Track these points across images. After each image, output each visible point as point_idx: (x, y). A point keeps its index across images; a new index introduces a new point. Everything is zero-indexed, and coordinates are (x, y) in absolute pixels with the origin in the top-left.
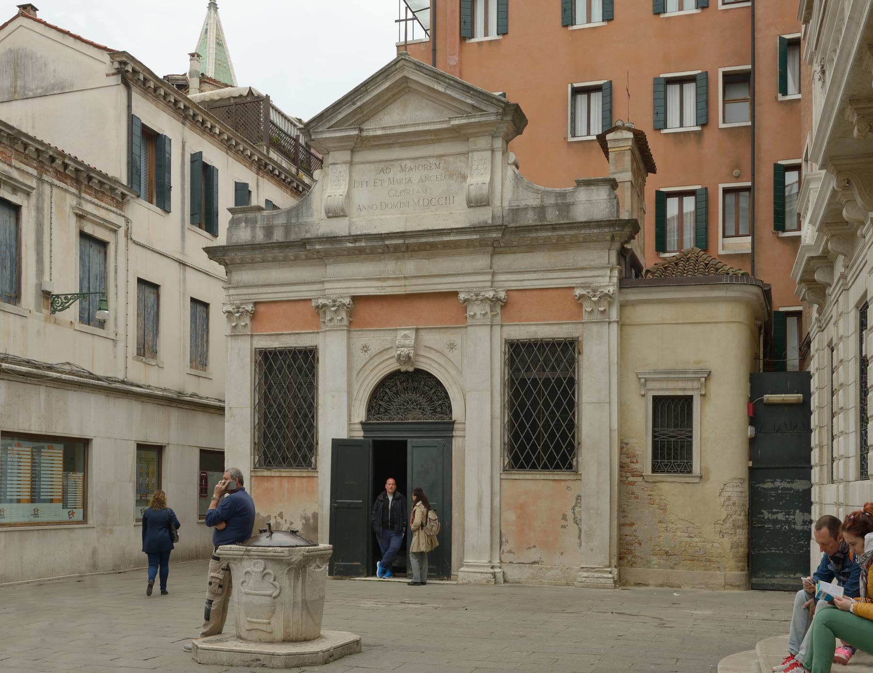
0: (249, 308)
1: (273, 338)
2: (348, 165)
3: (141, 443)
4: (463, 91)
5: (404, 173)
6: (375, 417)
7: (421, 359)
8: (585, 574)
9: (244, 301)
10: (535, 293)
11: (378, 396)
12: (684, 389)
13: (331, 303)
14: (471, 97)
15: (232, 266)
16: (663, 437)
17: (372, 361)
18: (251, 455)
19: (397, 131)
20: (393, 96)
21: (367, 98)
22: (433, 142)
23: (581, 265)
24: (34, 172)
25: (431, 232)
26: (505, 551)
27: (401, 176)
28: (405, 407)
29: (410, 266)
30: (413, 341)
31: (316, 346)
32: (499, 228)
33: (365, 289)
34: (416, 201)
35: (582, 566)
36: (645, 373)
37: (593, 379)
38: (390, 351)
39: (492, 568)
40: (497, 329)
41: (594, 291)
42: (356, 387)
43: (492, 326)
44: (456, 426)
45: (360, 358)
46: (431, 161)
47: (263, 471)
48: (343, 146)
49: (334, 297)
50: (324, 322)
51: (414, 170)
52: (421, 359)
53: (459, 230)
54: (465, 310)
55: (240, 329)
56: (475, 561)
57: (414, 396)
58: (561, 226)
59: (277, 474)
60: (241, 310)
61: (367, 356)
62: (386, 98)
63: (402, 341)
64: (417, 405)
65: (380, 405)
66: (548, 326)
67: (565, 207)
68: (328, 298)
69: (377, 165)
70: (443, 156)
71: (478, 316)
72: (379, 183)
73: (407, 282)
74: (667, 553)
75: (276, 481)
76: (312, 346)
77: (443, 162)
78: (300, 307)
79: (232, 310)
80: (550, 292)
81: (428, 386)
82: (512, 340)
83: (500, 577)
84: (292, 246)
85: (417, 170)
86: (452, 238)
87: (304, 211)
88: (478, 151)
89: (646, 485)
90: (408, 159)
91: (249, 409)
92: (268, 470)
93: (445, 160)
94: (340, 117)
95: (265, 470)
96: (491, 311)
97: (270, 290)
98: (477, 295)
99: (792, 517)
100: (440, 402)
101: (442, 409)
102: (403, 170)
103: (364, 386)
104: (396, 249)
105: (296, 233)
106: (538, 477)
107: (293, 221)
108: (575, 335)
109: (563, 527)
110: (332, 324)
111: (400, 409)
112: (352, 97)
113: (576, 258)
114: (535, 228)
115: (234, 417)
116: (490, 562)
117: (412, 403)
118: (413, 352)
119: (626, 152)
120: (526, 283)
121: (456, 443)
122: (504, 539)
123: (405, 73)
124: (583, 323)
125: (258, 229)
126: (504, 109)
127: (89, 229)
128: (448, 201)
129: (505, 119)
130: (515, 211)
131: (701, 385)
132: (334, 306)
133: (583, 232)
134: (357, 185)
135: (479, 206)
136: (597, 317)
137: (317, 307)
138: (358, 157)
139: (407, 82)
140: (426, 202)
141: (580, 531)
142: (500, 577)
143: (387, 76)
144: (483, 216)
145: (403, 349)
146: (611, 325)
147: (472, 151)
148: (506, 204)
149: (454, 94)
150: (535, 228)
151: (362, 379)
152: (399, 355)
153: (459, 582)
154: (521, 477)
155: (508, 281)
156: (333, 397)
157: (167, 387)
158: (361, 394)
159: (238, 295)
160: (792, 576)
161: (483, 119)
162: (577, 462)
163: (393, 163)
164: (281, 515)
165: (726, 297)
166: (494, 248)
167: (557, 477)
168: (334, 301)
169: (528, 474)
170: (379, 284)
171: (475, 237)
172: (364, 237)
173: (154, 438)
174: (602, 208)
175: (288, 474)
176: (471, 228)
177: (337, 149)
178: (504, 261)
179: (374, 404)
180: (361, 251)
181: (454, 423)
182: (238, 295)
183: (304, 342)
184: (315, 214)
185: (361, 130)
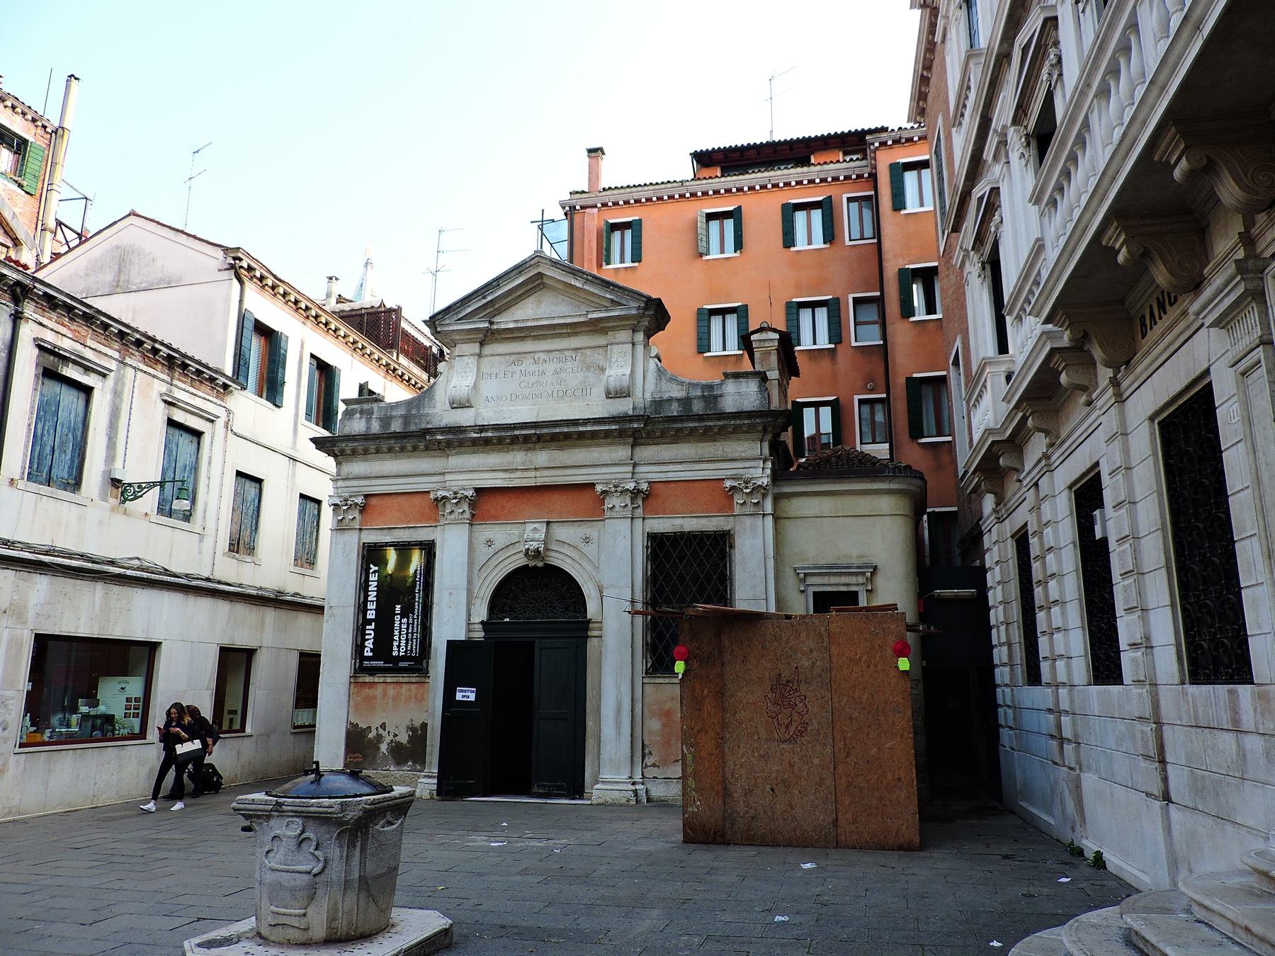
0: (360, 500)
1: (385, 532)
2: (476, 357)
7: (552, 554)
9: (353, 494)
12: (848, 585)
18: (352, 659)
19: (529, 324)
20: (527, 291)
21: (500, 292)
22: (569, 335)
23: (731, 456)
24: (116, 355)
27: (533, 368)
34: (550, 393)
38: (517, 544)
39: (633, 784)
40: (638, 522)
41: (746, 483)
42: (477, 583)
43: (632, 518)
44: (591, 625)
45: (483, 553)
46: (567, 353)
48: (472, 339)
49: (455, 489)
50: (443, 515)
52: (552, 554)
60: (349, 502)
61: (491, 551)
68: (448, 490)
69: (507, 357)
70: (580, 349)
71: (617, 508)
72: (510, 375)
73: (538, 474)
75: (380, 689)
77: (579, 355)
78: (417, 499)
80: (697, 483)
83: (642, 794)
87: (426, 402)
90: (542, 351)
94: (469, 310)
96: (632, 504)
98: (615, 487)
103: (487, 583)
104: (526, 439)
105: (416, 424)
108: (726, 528)
110: (452, 517)
111: (528, 607)
112: (483, 291)
116: (630, 778)
120: (670, 475)
121: (592, 644)
122: (647, 751)
123: (540, 270)
124: (735, 516)
126: (646, 303)
127: (179, 416)
128: (584, 392)
129: (646, 313)
130: (658, 404)
131: (867, 579)
132: (455, 498)
134: (485, 376)
136: (752, 510)
137: (436, 499)
138: (488, 349)
139: (542, 279)
140: (561, 394)
142: (642, 794)
144: (623, 407)
145: (531, 543)
148: (648, 396)
152: (528, 549)
155: (650, 473)
156: (451, 594)
158: (482, 591)
161: (623, 313)
164: (383, 726)
166: (635, 439)
170: (507, 475)
171: (614, 427)
173: (242, 640)
174: (752, 400)
175: (395, 680)
177: (464, 342)
178: (645, 453)
181: (589, 621)
184: (439, 405)
185: (491, 323)
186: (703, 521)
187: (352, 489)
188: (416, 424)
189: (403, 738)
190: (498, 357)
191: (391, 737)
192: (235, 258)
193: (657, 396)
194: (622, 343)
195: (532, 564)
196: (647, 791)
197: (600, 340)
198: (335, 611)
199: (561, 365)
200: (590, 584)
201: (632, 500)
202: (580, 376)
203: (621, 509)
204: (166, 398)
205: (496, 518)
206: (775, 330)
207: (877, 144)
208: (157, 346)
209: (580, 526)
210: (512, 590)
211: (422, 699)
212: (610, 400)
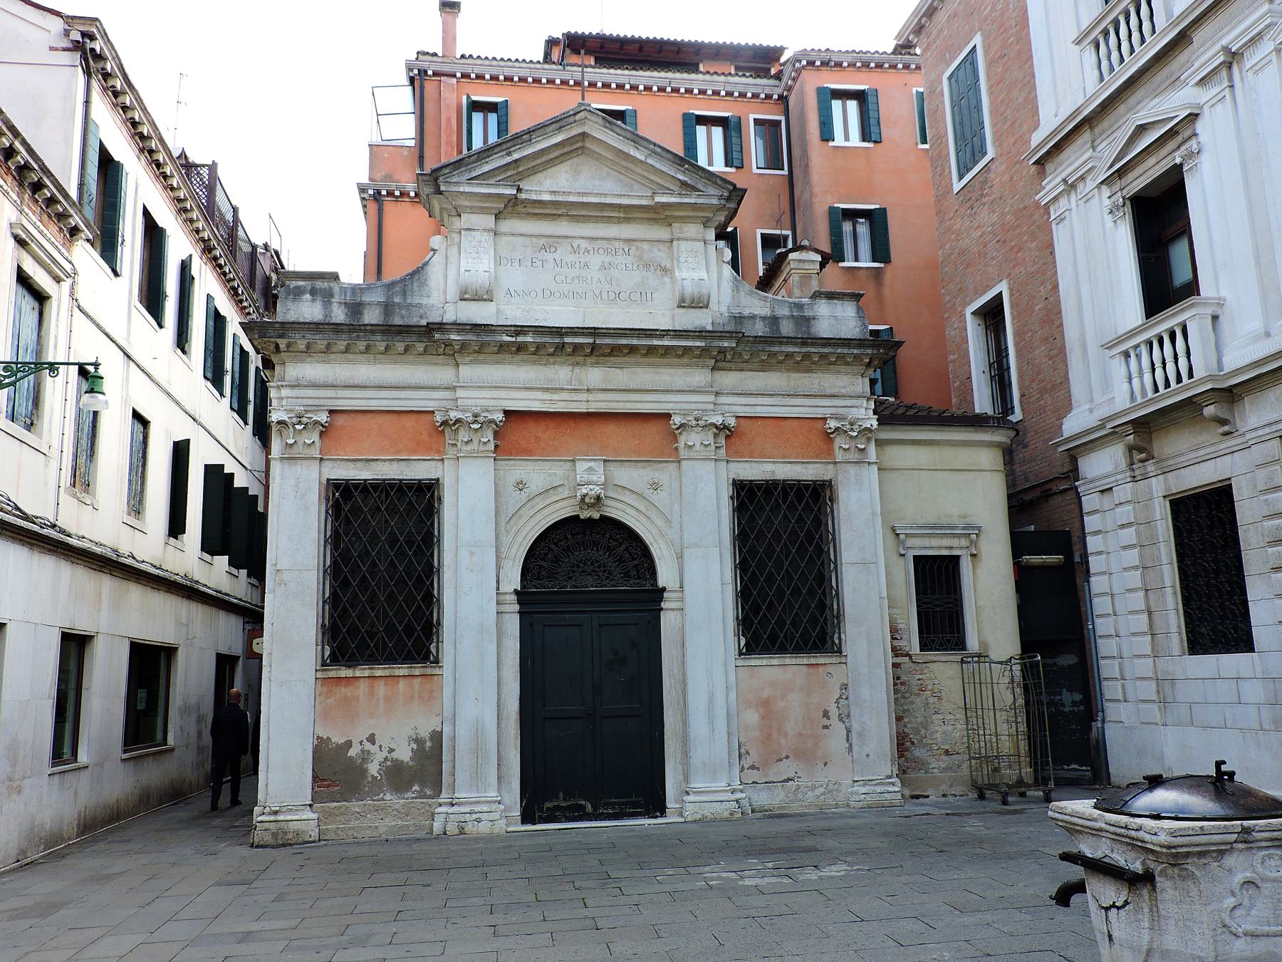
1: (360, 464)
3: (67, 631)
4: (674, 162)
7: (610, 502)
8: (864, 790)
9: (309, 408)
10: (770, 422)
11: (537, 553)
12: (951, 548)
13: (471, 418)
14: (684, 172)
15: (288, 354)
18: (317, 645)
19: (572, 199)
21: (529, 151)
22: (619, 220)
23: (829, 391)
25: (637, 332)
26: (746, 767)
27: (571, 258)
29: (594, 375)
31: (438, 480)
32: (734, 335)
33: (525, 402)
34: (597, 293)
35: (856, 779)
36: (906, 528)
37: (853, 533)
38: (560, 489)
41: (852, 424)
42: (506, 540)
44: (666, 595)
46: (617, 244)
47: (340, 669)
48: (486, 208)
49: (477, 410)
51: (591, 252)
52: (610, 502)
53: (678, 333)
54: (675, 439)
55: (299, 450)
56: (709, 785)
58: (814, 341)
59: (367, 673)
60: (304, 420)
61: (524, 496)
62: (552, 156)
63: (586, 476)
66: (789, 465)
67: (805, 322)
68: (463, 411)
69: (535, 240)
71: (698, 447)
73: (591, 397)
74: (947, 752)
75: (363, 687)
76: (431, 480)
77: (633, 248)
78: (409, 422)
79: (287, 419)
80: (788, 422)
82: (742, 481)
83: (745, 803)
84: (407, 332)
85: (596, 254)
86: (666, 342)
87: (416, 288)
88: (687, 240)
89: (913, 665)
91: (315, 573)
92: (349, 667)
93: (637, 247)
94: (486, 168)
97: (358, 393)
99: (1058, 697)
101: (638, 572)
103: (519, 539)
104: (577, 348)
105: (403, 317)
106: (788, 661)
107: (397, 300)
109: (826, 727)
110: (469, 448)
112: (509, 144)
113: (822, 383)
114: (779, 340)
115: (285, 584)
120: (758, 409)
121: (668, 621)
123: (586, 129)
124: (835, 463)
125: (335, 305)
126: (730, 192)
129: (728, 205)
131: (972, 542)
132: (475, 422)
133: (839, 351)
135: (693, 307)
136: (853, 456)
137: (445, 423)
138: (508, 225)
139: (583, 141)
140: (612, 296)
143: (561, 127)
149: (657, 165)
150: (779, 340)
152: (585, 496)
153: (689, 819)
154: (765, 662)
155: (743, 406)
156: (472, 554)
157: (102, 542)
158: (514, 550)
159: (296, 398)
160: (1066, 767)
161: (700, 201)
162: (840, 639)
163: (560, 240)
164: (371, 739)
165: (991, 442)
167: (813, 661)
168: (476, 416)
169: (774, 658)
170: (547, 396)
171: (698, 344)
172: (532, 329)
173: (82, 625)
175: (387, 673)
176: (696, 331)
177: (474, 210)
178: (729, 379)
180: (521, 348)
181: (664, 589)
182: (296, 398)
183: (418, 471)
184: (435, 294)
185: (519, 190)
186: (798, 468)
187: (305, 402)
188: (403, 317)
189: (404, 754)
190: (520, 238)
191: (385, 754)
192: (84, 34)
193: (736, 311)
194: (692, 240)
195: (584, 515)
197: (661, 233)
198: (286, 576)
199: (609, 258)
200: (661, 541)
201: (716, 435)
203: (703, 448)
204: (20, 232)
205: (528, 452)
206: (817, 251)
207: (804, 63)
208: (17, 145)
209: (644, 468)
210: (550, 549)
211: (431, 697)
212: (682, 310)
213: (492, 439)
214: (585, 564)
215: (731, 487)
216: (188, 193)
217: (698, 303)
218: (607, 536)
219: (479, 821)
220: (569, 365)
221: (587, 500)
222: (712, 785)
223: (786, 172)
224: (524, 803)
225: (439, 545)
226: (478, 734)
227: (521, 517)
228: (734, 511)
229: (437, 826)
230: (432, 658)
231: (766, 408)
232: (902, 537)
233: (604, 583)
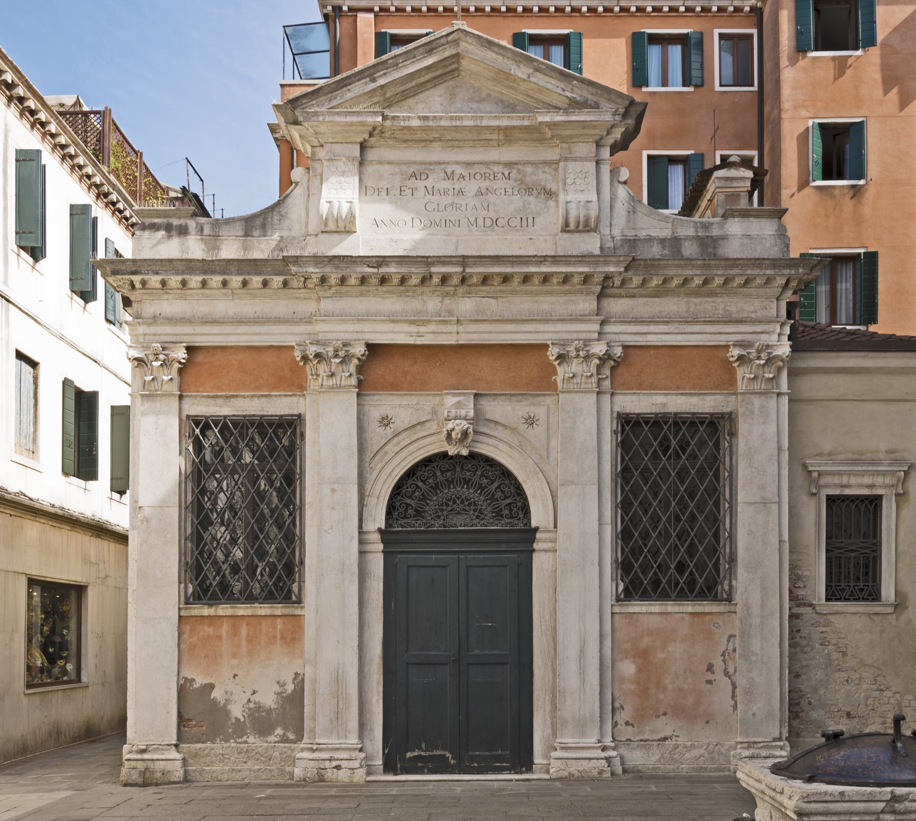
0: (181, 354)
5: (451, 181)
6: (399, 522)
11: (404, 491)
16: (863, 551)
17: (396, 440)
18: (180, 582)
27: (447, 184)
28: (449, 508)
30: (472, 411)
33: (390, 335)
34: (472, 220)
37: (754, 470)
38: (428, 424)
40: (607, 398)
43: (598, 393)
44: (538, 535)
45: (377, 435)
51: (467, 178)
57: (463, 491)
61: (389, 432)
64: (469, 505)
65: (408, 505)
69: (404, 168)
81: (487, 478)
90: (457, 163)
92: (211, 605)
95: (206, 607)
100: (508, 501)
101: (511, 510)
102: (449, 177)
111: (442, 510)
116: (599, 741)
117: (462, 502)
118: (472, 426)
119: (742, 194)
121: (541, 563)
122: (617, 705)
128: (525, 223)
141: (734, 687)
142: (617, 762)
146: (780, 398)
147: (566, 159)
148: (617, 232)
151: (380, 465)
158: (378, 488)
170: (414, 329)
179: (398, 504)
181: (536, 529)
195: (452, 451)
196: (622, 757)
199: (487, 183)
202: (517, 201)
210: (418, 487)
211: (293, 639)
213: (354, 374)
214: (454, 502)
215: (615, 422)
216: (70, 138)
217: (586, 227)
218: (479, 473)
219: (338, 767)
220: (439, 296)
221: (454, 435)
222: (581, 740)
223: (755, 88)
224: (386, 751)
225: (301, 481)
226: (338, 679)
227: (386, 453)
228: (617, 446)
229: (298, 772)
230: (294, 598)
231: (660, 336)
232: (815, 475)
233: (474, 522)
